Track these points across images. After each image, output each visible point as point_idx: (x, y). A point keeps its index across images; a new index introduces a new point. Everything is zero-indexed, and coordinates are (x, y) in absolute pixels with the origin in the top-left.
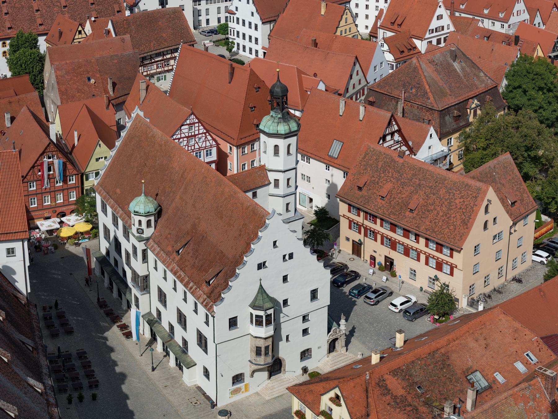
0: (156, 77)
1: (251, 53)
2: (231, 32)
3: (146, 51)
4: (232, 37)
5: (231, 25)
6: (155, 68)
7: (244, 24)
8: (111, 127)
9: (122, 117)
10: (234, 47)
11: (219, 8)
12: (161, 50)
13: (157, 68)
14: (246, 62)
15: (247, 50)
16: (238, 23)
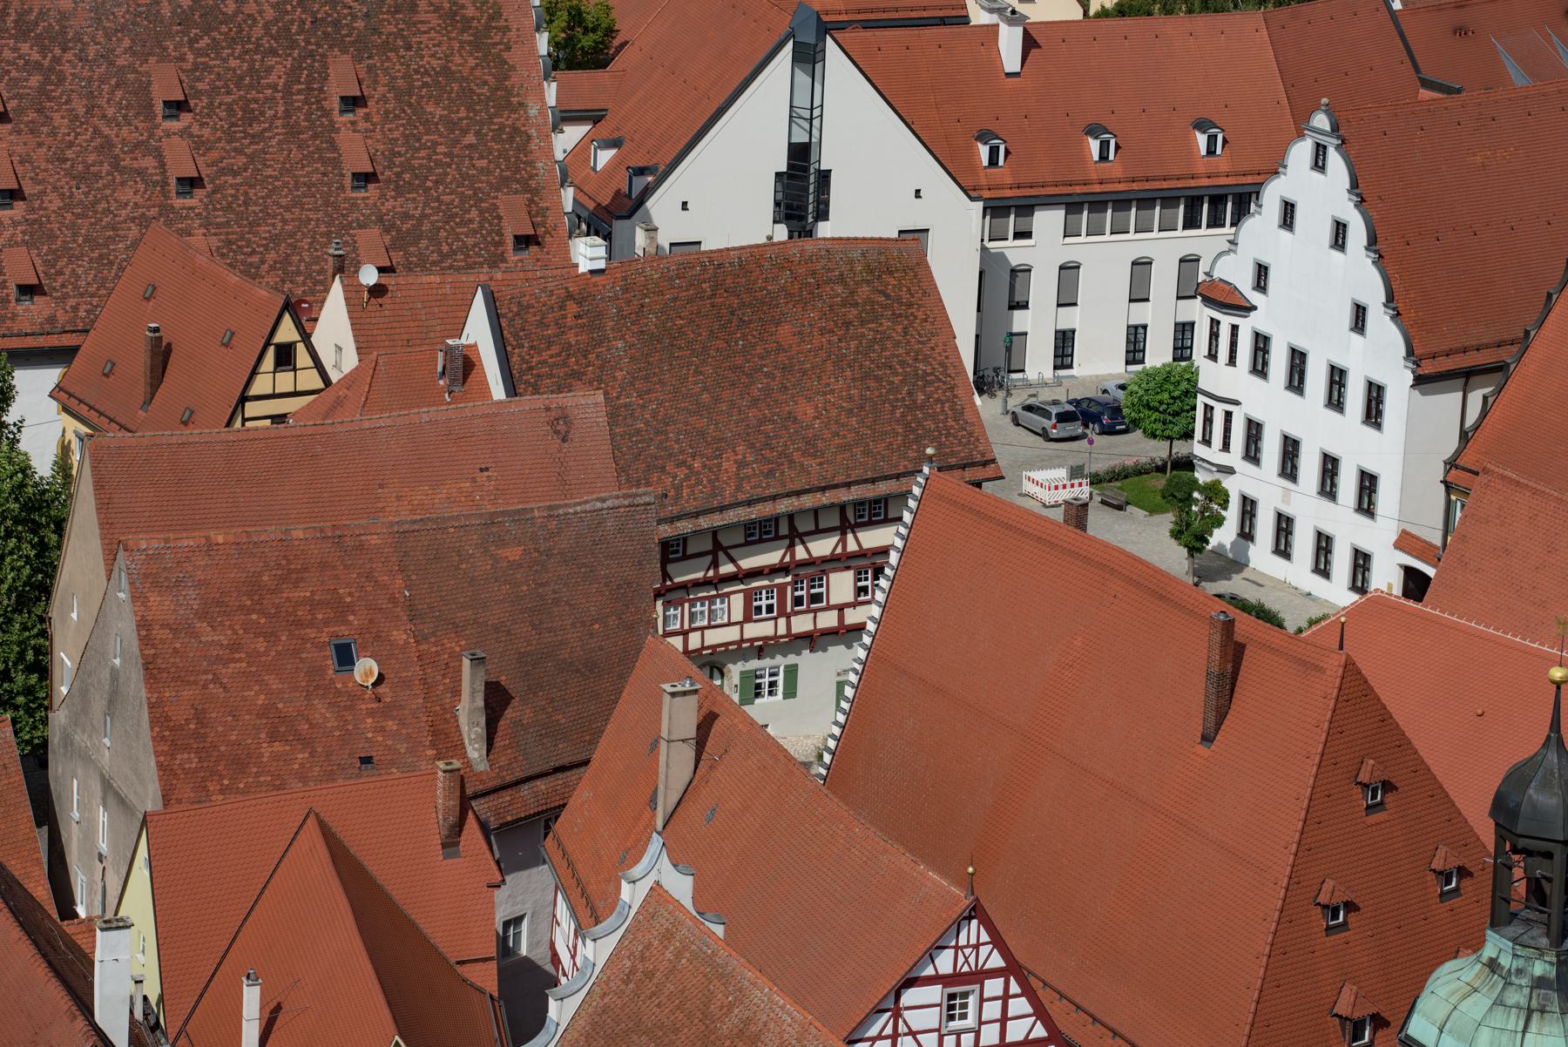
0: (735, 670)
1: (1322, 568)
2: (1208, 421)
3: (691, 507)
4: (1213, 454)
5: (1214, 377)
6: (738, 615)
7: (1296, 381)
8: (464, 971)
9: (526, 908)
10: (1219, 521)
11: (1141, 266)
12: (783, 506)
13: (747, 619)
14: (1293, 620)
15: (1303, 544)
16: (1260, 369)
